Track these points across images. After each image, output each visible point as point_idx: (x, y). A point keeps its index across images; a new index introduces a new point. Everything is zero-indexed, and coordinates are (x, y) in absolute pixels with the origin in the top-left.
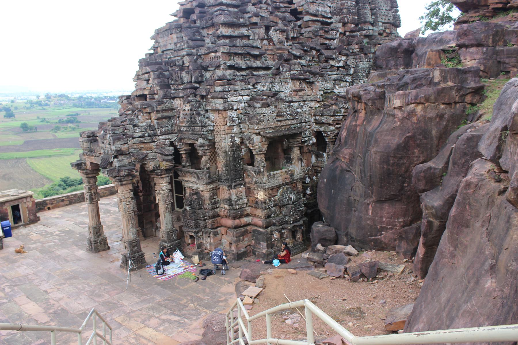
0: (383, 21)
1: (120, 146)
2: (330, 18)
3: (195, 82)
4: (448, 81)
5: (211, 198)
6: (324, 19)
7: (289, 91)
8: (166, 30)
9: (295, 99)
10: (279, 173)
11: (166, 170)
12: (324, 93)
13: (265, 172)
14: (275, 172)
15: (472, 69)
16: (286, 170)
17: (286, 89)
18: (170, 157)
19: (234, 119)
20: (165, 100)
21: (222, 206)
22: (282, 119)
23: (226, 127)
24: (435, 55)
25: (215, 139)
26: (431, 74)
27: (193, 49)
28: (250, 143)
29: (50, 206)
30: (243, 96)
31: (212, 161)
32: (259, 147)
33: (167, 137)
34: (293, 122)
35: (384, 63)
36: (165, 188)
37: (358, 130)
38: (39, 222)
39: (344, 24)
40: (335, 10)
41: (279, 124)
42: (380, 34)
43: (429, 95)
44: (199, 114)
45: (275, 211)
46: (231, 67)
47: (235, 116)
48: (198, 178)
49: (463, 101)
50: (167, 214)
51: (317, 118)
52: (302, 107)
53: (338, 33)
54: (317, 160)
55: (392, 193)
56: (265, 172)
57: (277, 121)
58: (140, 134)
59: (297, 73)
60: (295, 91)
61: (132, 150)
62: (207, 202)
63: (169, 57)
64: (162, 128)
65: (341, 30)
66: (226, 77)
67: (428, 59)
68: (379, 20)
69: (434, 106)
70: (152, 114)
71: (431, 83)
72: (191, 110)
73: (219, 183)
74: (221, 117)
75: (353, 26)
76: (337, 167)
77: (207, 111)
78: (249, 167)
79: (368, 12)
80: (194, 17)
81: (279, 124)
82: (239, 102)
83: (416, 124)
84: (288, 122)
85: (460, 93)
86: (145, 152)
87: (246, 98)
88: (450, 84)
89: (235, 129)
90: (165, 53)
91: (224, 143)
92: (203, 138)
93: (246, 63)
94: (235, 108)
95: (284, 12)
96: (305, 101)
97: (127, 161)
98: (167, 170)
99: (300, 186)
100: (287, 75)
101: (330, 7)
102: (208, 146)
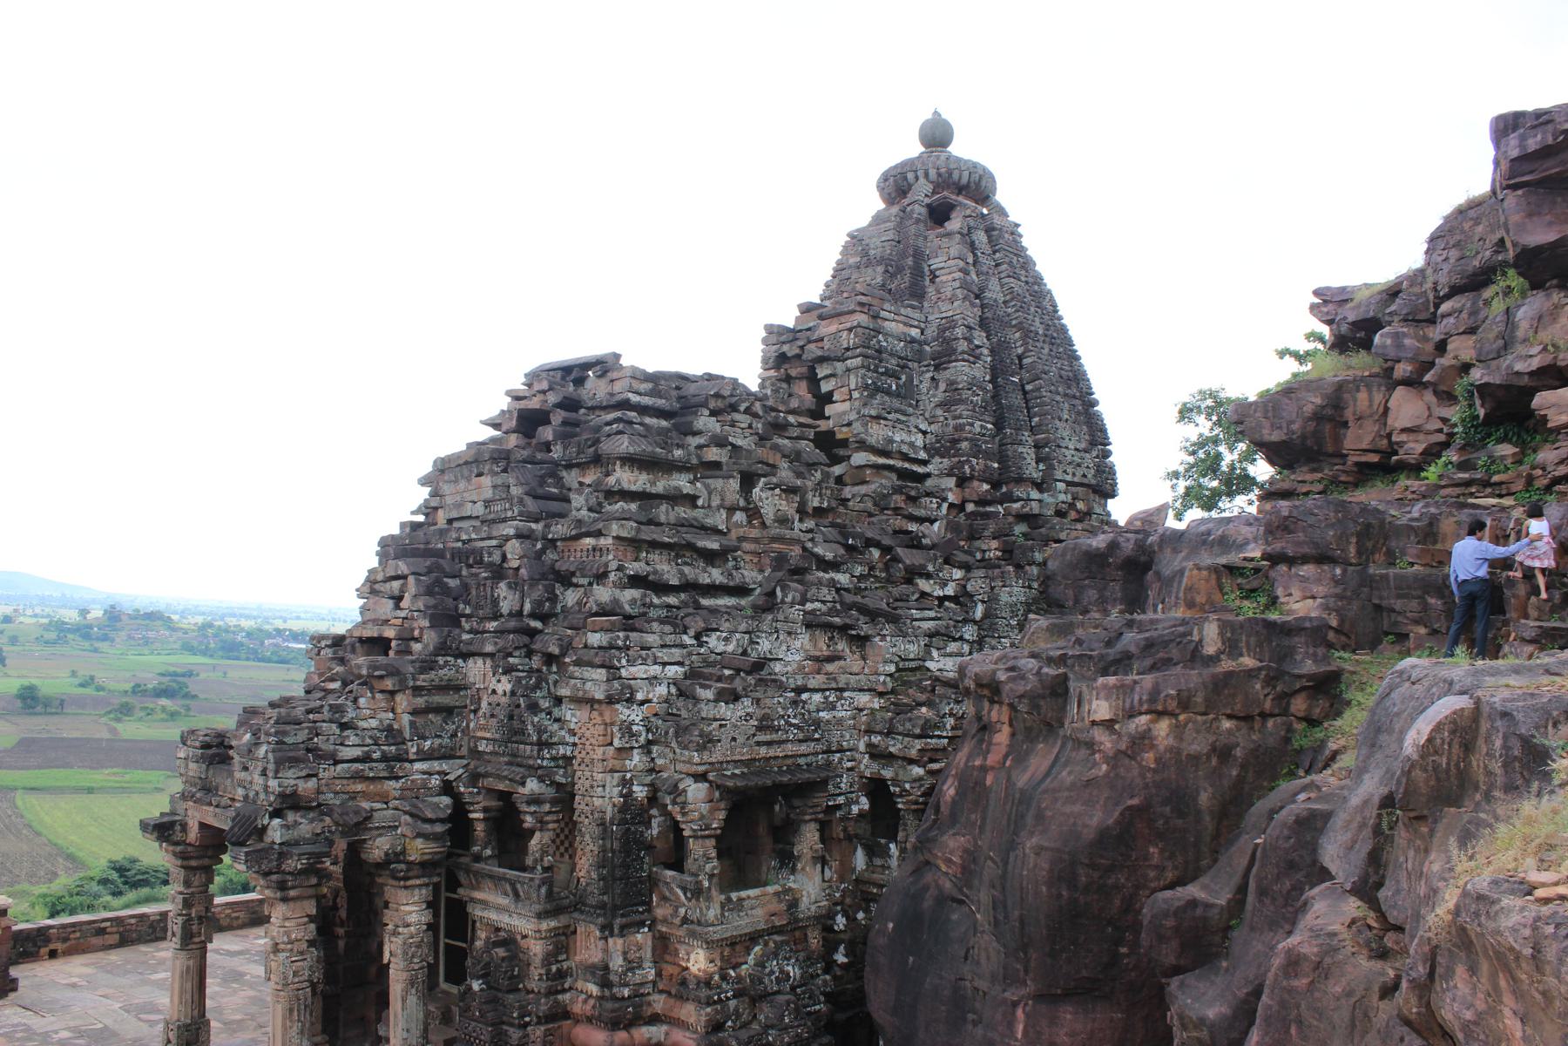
0: (1069, 478)
1: (293, 782)
2: (924, 463)
3: (533, 615)
4: (1241, 655)
5: (549, 959)
6: (907, 465)
7: (797, 658)
8: (466, 463)
9: (812, 683)
10: (756, 898)
11: (423, 864)
12: (898, 670)
13: (714, 893)
14: (743, 894)
15: (1307, 624)
16: (777, 888)
17: (791, 652)
18: (439, 828)
19: (635, 728)
20: (441, 660)
21: (580, 985)
22: (774, 737)
23: (610, 750)
24: (1207, 581)
25: (574, 784)
26: (1195, 632)
27: (536, 521)
28: (674, 803)
29: (59, 946)
30: (665, 664)
31: (562, 849)
32: (702, 817)
33: (436, 765)
34: (803, 748)
35: (1070, 593)
36: (413, 918)
37: (988, 782)
38: (12, 995)
39: (962, 482)
40: (938, 441)
42: (1060, 514)
43: (1189, 690)
44: (534, 708)
45: (736, 1010)
46: (637, 581)
47: (637, 720)
48: (517, 895)
49: (1285, 712)
50: (412, 1000)
51: (876, 739)
52: (832, 707)
53: (945, 505)
54: (870, 863)
55: (1084, 973)
56: (714, 893)
57: (759, 744)
58: (357, 752)
60: (816, 659)
61: (329, 797)
62: (536, 972)
63: (464, 537)
64: (424, 738)
65: (951, 498)
66: (622, 607)
67: (1189, 589)
68: (1059, 474)
69: (1205, 722)
70: (399, 697)
71: (1195, 656)
72: (513, 693)
73: (576, 915)
74: (599, 720)
75: (986, 487)
76: (926, 888)
77: (558, 701)
78: (670, 873)
79: (1029, 454)
80: (546, 433)
81: (763, 751)
82: (653, 680)
83: (1155, 771)
84: (790, 749)
85: (1274, 687)
86: (366, 805)
87: (672, 671)
88: (1248, 662)
89: (637, 760)
90: (456, 524)
91: (600, 795)
92: (541, 780)
93: (682, 573)
94: (640, 696)
95: (797, 438)
96: (842, 690)
97: (309, 828)
98: (426, 866)
99: (815, 940)
100: (796, 613)
101: (924, 433)
102: (554, 802)
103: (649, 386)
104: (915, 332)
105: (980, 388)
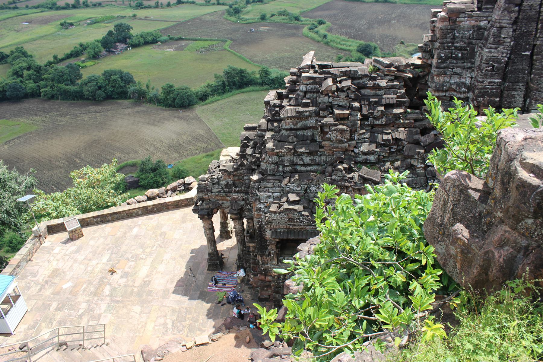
22: (295, 223)
30: (273, 193)
41: (291, 227)
58: (218, 190)
59: (339, 178)
64: (236, 187)
81: (291, 227)
82: (270, 197)
86: (220, 202)
87: (276, 194)
103: (312, 81)
104: (482, 24)
105: (497, 62)
